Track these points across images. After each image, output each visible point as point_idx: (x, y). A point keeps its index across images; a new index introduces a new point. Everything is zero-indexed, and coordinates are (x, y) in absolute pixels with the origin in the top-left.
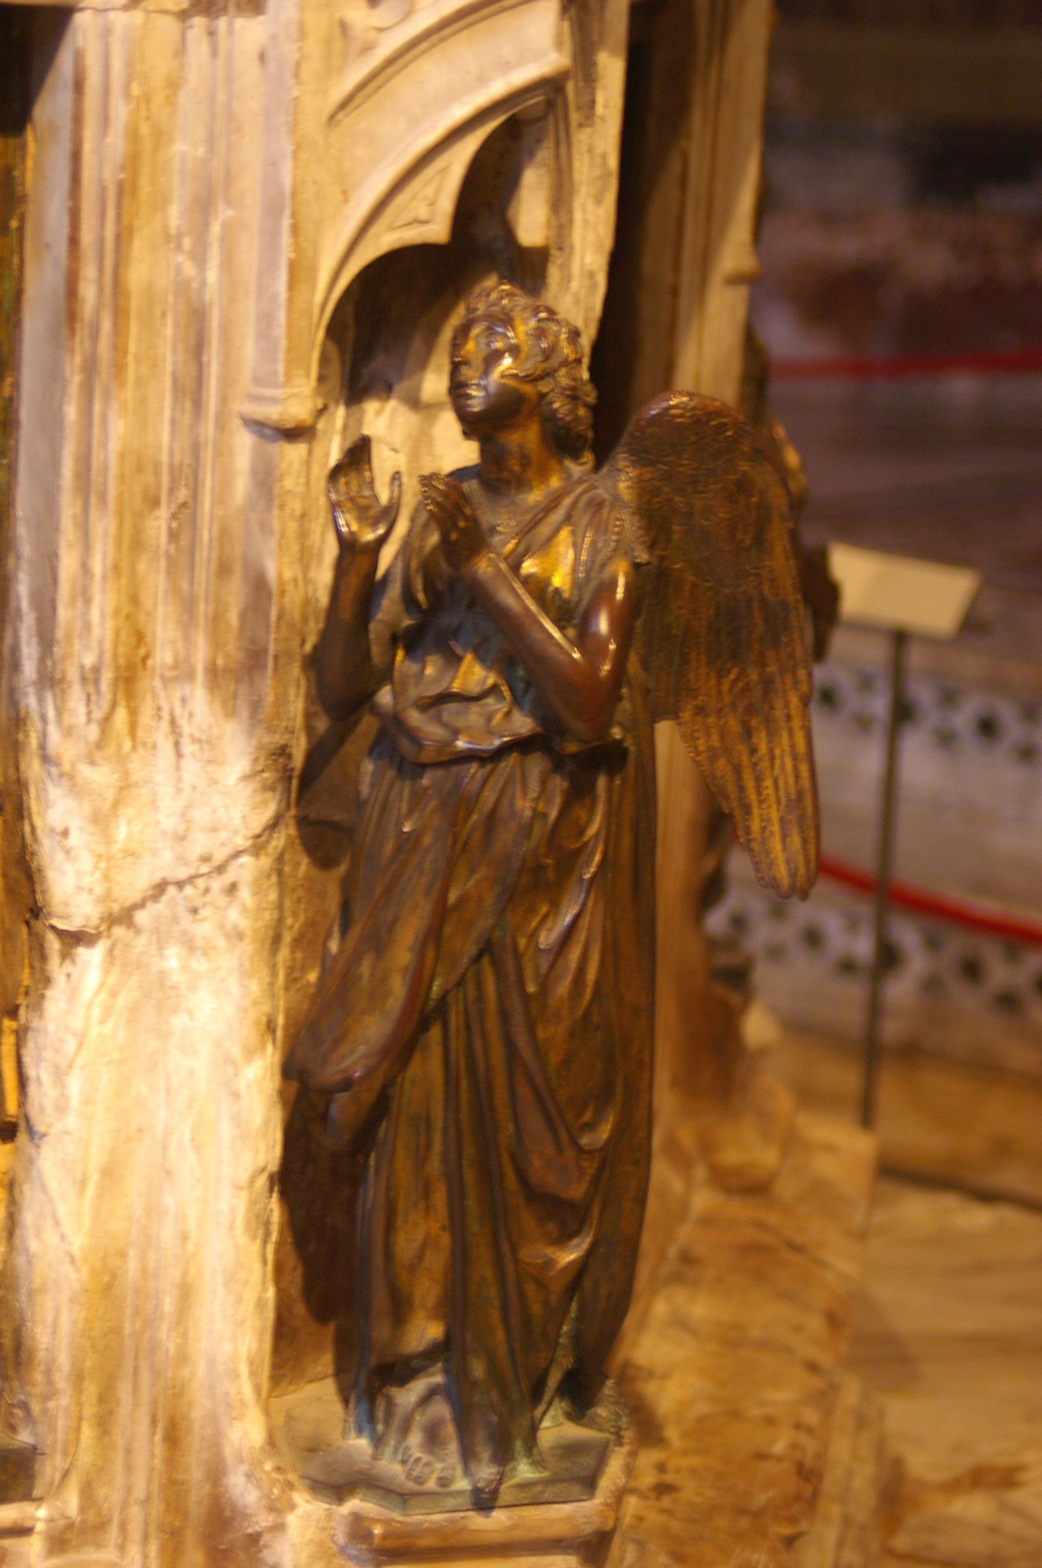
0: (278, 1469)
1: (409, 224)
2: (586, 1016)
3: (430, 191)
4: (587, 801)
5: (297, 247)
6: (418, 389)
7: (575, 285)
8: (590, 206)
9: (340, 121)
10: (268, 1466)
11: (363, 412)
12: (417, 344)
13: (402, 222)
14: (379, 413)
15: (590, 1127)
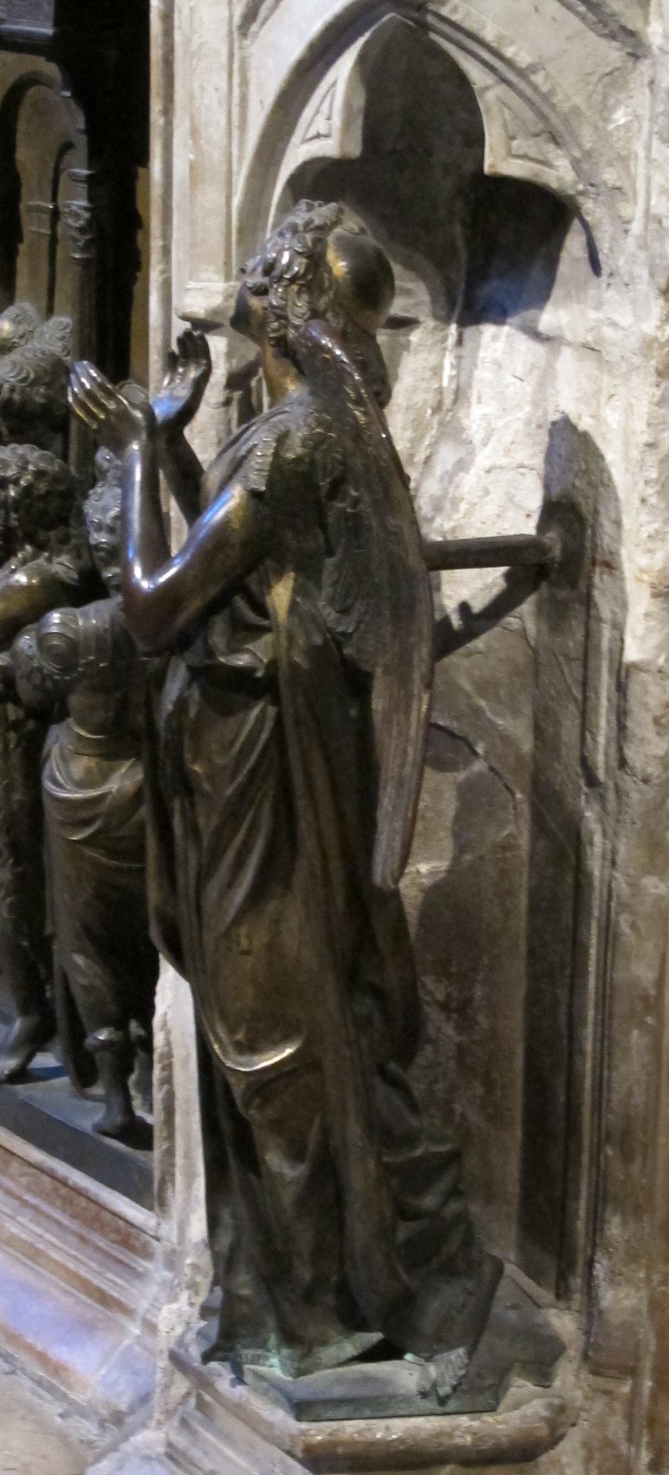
0: (194, 1267)
1: (318, 136)
2: (226, 934)
3: (325, 107)
4: (232, 721)
5: (197, 149)
6: (536, 320)
7: (636, 228)
8: (656, 143)
9: (257, 33)
10: (188, 1261)
11: (481, 333)
12: (536, 272)
13: (309, 135)
14: (495, 338)
15: (251, 1047)
